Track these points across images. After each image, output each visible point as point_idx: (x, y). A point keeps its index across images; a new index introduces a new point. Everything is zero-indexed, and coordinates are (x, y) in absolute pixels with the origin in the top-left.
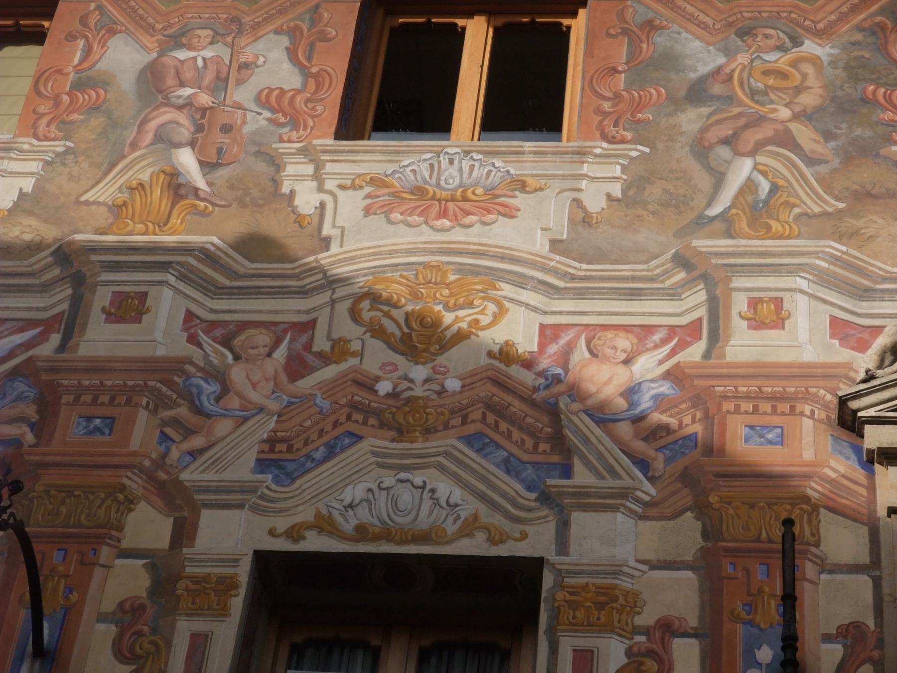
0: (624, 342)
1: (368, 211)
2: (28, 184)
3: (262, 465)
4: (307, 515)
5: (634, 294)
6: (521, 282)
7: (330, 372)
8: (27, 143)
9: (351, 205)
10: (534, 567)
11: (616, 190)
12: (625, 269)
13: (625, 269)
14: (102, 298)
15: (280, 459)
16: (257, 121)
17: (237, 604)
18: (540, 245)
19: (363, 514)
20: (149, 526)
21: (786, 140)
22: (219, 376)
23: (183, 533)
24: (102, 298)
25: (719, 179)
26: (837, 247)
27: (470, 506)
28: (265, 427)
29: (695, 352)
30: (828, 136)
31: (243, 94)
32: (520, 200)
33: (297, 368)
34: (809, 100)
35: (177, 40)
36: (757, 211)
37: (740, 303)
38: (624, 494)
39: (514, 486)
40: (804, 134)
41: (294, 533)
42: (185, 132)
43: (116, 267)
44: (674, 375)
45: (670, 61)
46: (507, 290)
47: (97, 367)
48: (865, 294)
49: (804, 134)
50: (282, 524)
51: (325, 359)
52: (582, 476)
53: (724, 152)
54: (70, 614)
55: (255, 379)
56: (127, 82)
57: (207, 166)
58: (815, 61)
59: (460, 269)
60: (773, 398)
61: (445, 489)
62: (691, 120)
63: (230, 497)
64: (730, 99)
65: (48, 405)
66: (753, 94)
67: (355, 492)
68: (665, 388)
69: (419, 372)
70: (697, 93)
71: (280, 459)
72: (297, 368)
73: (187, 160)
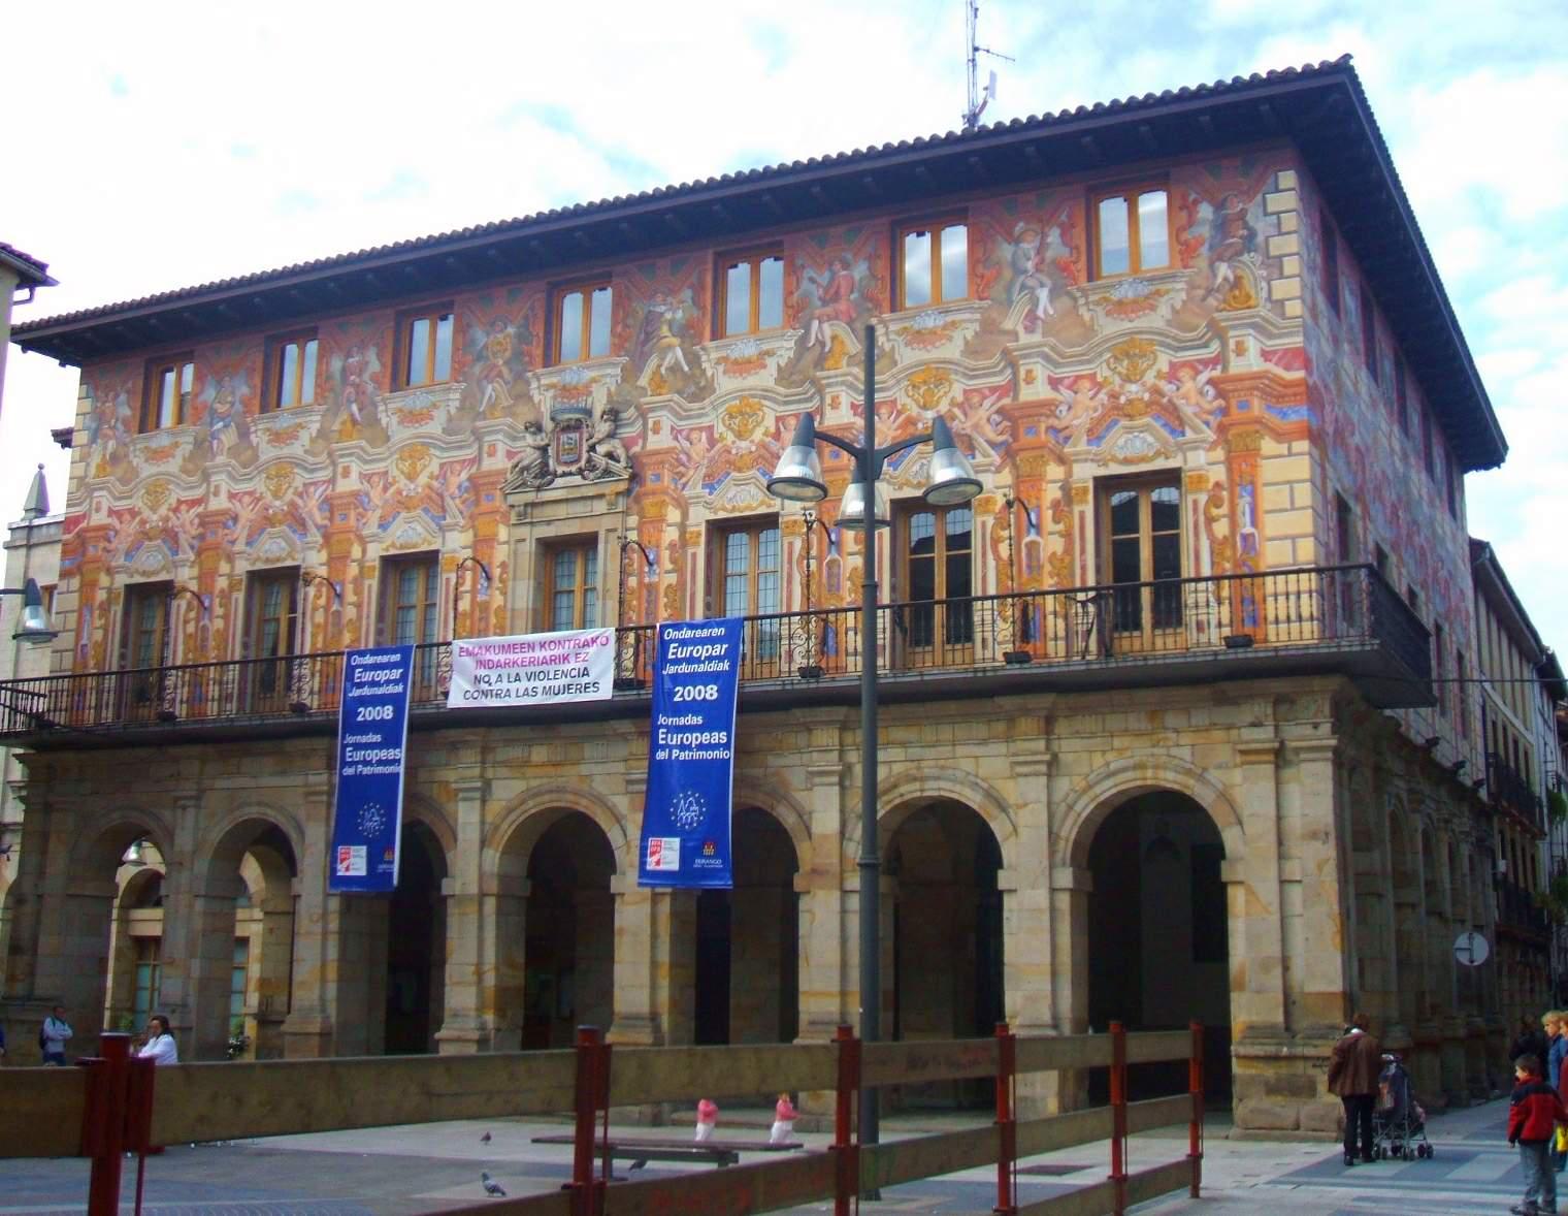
0: (458, 467)
1: (399, 423)
2: (318, 425)
3: (381, 526)
4: (389, 543)
5: (460, 448)
6: (435, 447)
7: (392, 490)
8: (317, 408)
9: (395, 420)
10: (436, 552)
11: (457, 404)
12: (459, 438)
13: (459, 438)
14: (340, 470)
15: (383, 525)
16: (370, 387)
17: (377, 573)
18: (440, 431)
19: (402, 541)
20: (356, 552)
21: (500, 375)
22: (367, 494)
23: (364, 552)
24: (340, 470)
25: (483, 394)
26: (509, 420)
27: (425, 534)
28: (379, 513)
29: (474, 470)
30: (511, 370)
31: (366, 377)
32: (435, 413)
33: (385, 489)
34: (508, 354)
35: (349, 355)
36: (492, 406)
37: (485, 449)
38: (456, 524)
39: (433, 525)
40: (505, 371)
41: (387, 550)
42: (353, 397)
43: (342, 456)
44: (470, 479)
45: (473, 342)
46: (432, 451)
47: (341, 496)
48: (514, 439)
49: (505, 371)
50: (384, 546)
51: (392, 485)
52: (449, 520)
53: (485, 382)
54: (343, 584)
55: (376, 496)
56: (338, 376)
57: (360, 410)
58: (508, 335)
59: (423, 444)
60: (493, 483)
61: (419, 529)
62: (477, 369)
63: (375, 538)
64: (487, 358)
65: (332, 512)
66: (494, 354)
67: (399, 533)
68: (467, 484)
69: (412, 486)
70: (479, 358)
71: (383, 525)
72: (385, 489)
73: (355, 408)
